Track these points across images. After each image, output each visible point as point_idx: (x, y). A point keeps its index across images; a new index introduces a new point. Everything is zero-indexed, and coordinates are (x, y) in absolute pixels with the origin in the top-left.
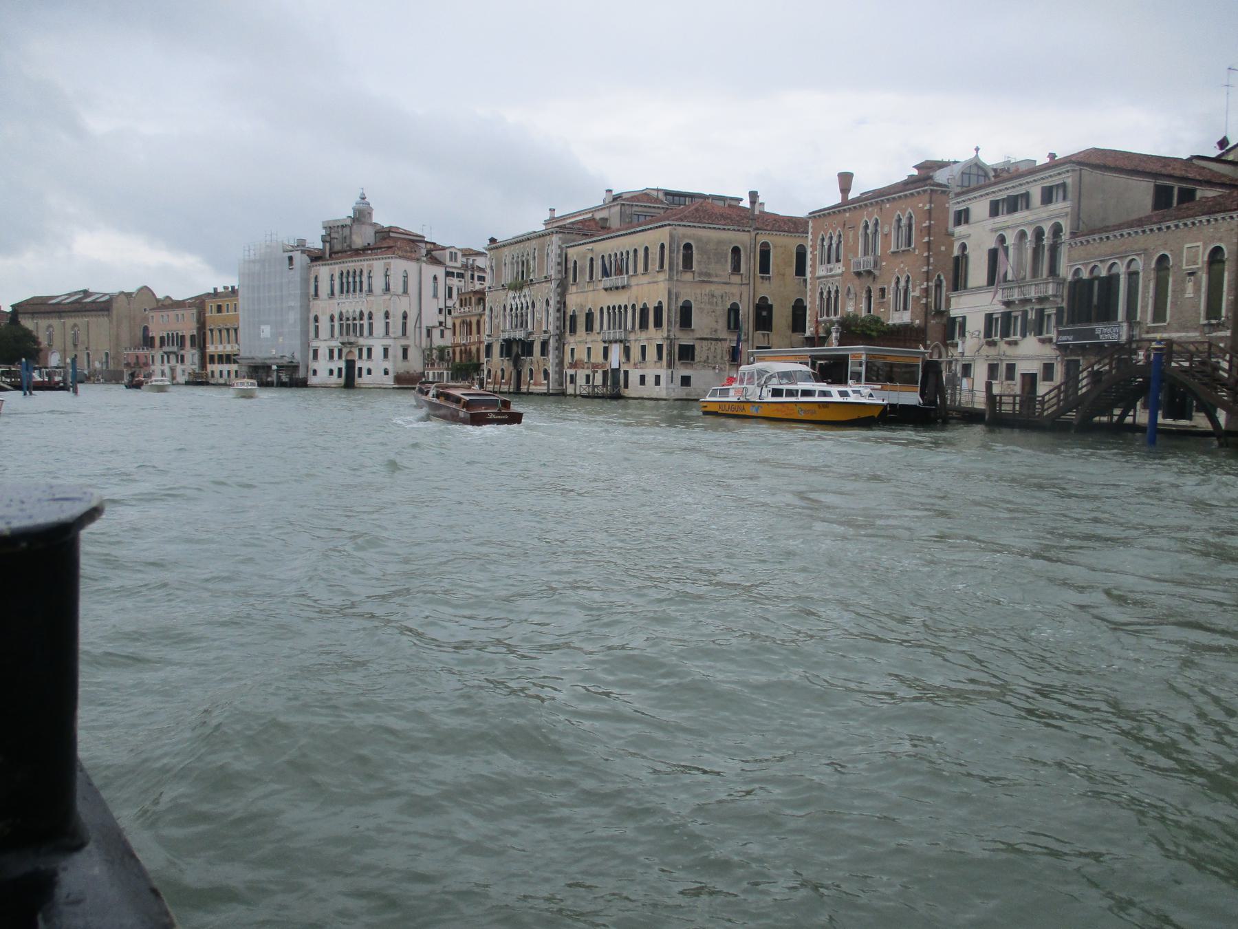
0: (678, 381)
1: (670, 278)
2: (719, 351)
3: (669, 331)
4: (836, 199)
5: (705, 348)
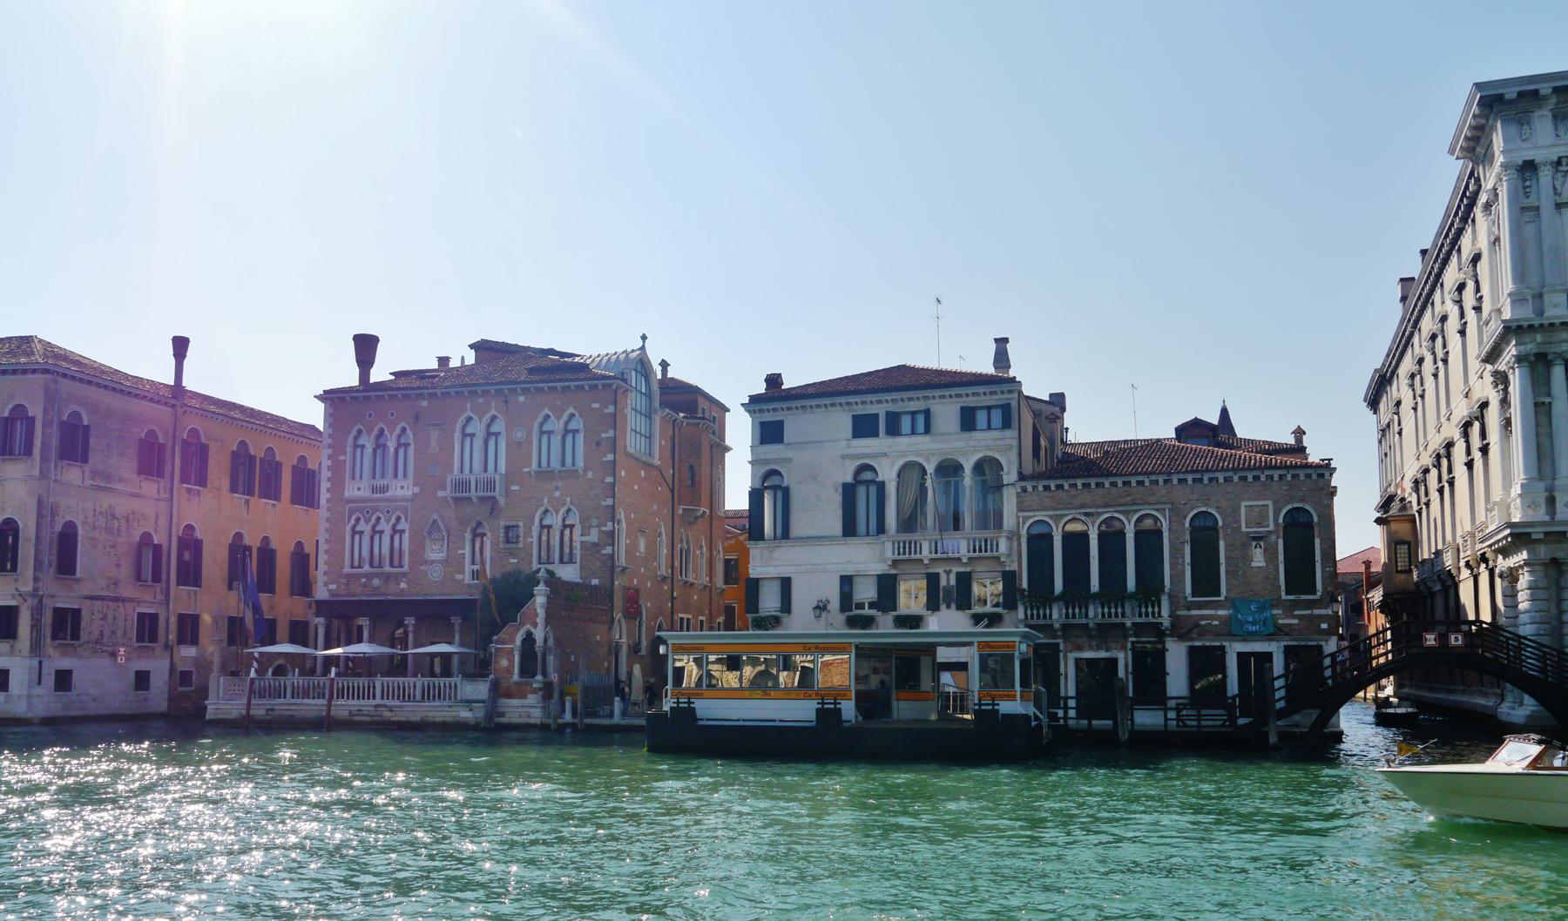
0: (49, 680)
1: (44, 475)
2: (120, 622)
3: (36, 580)
4: (351, 378)
5: (98, 616)
